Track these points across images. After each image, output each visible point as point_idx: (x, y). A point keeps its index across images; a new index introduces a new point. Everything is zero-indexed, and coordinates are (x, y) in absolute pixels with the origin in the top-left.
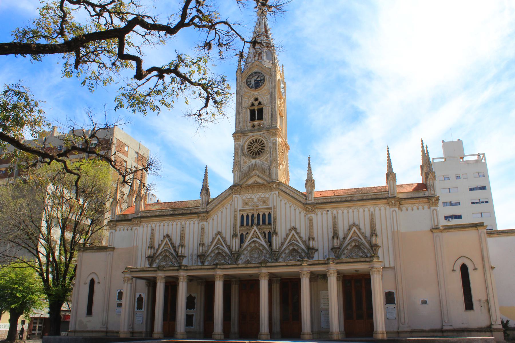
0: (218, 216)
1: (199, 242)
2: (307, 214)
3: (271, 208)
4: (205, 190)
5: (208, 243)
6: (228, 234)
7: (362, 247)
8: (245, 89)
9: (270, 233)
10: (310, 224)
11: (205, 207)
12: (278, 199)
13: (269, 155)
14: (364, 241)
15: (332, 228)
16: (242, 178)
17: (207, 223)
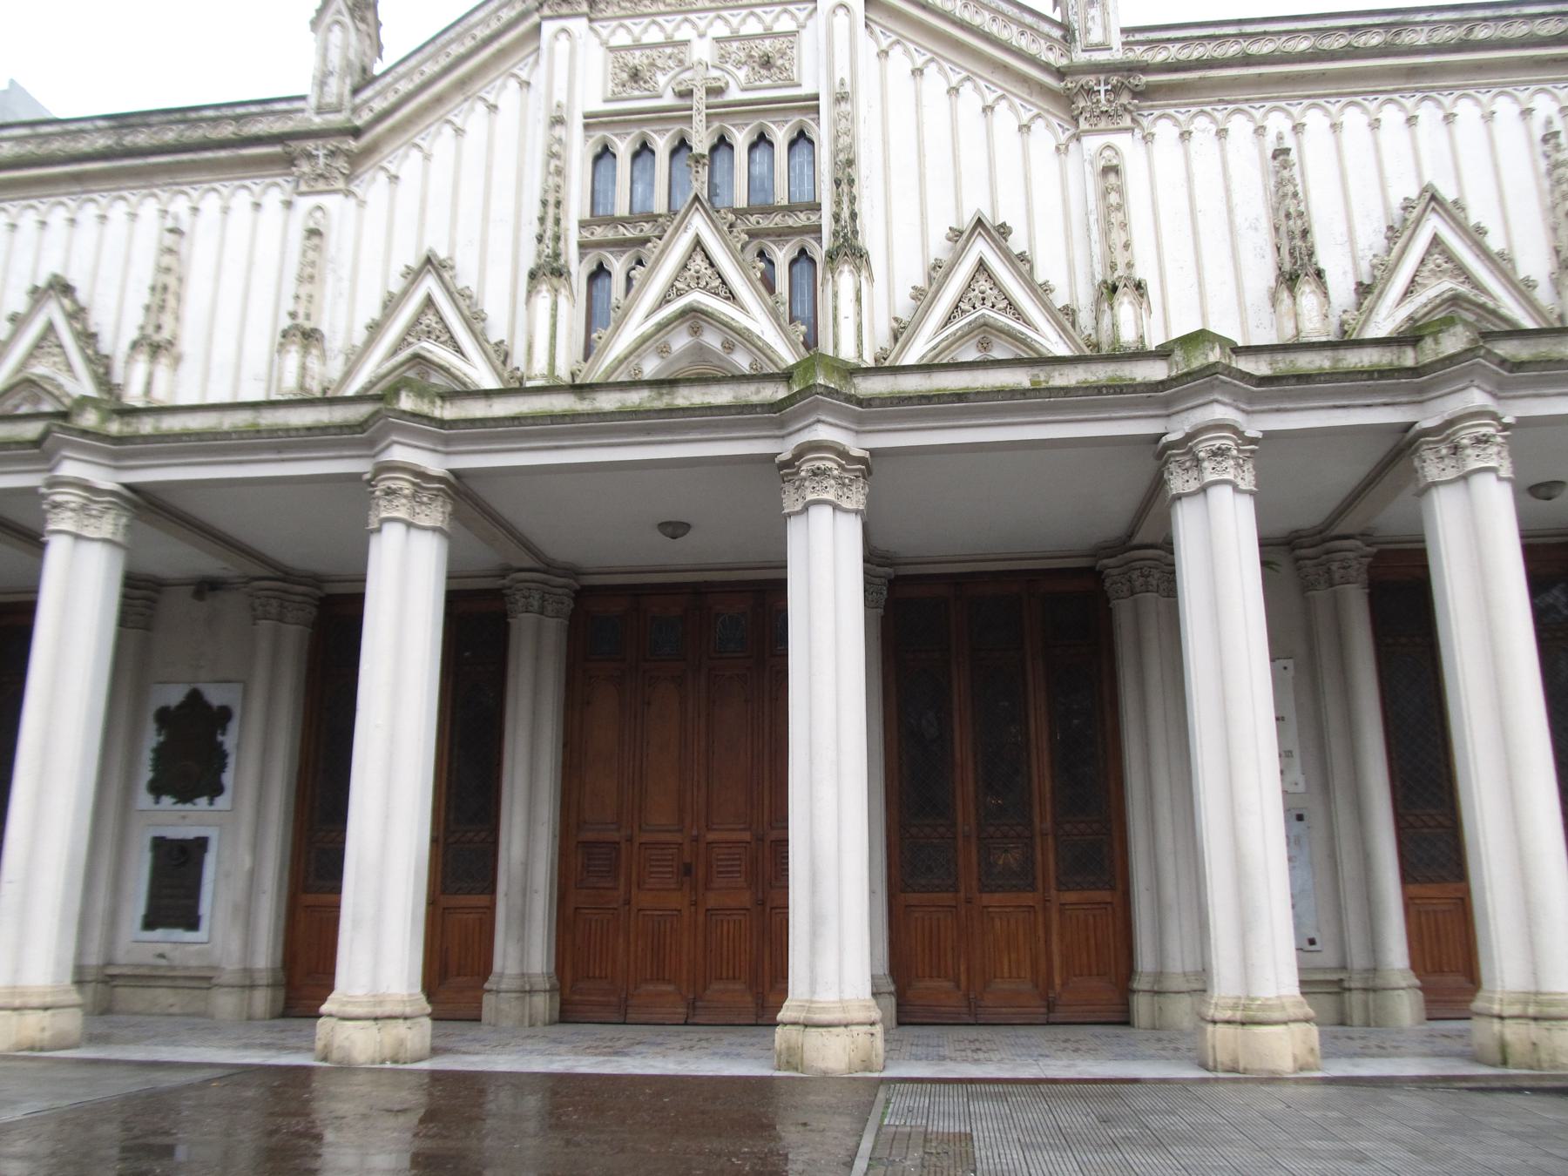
0: (427, 157)
1: (286, 322)
2: (1077, 138)
3: (816, 97)
5: (350, 330)
10: (1106, 192)
11: (341, 96)
12: (867, 47)
15: (1265, 225)
17: (352, 202)
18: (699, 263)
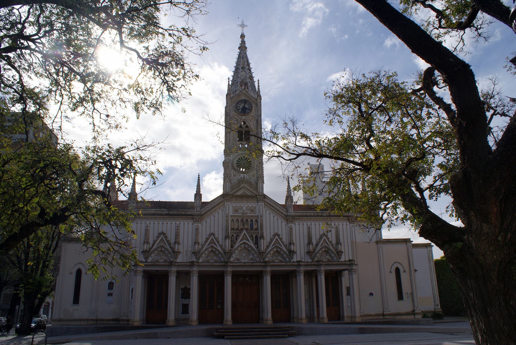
4: (198, 195)
5: (202, 242)
6: (220, 236)
7: (330, 252)
8: (233, 112)
9: (256, 237)
13: (255, 172)
14: (331, 248)
16: (232, 188)
18: (245, 236)
